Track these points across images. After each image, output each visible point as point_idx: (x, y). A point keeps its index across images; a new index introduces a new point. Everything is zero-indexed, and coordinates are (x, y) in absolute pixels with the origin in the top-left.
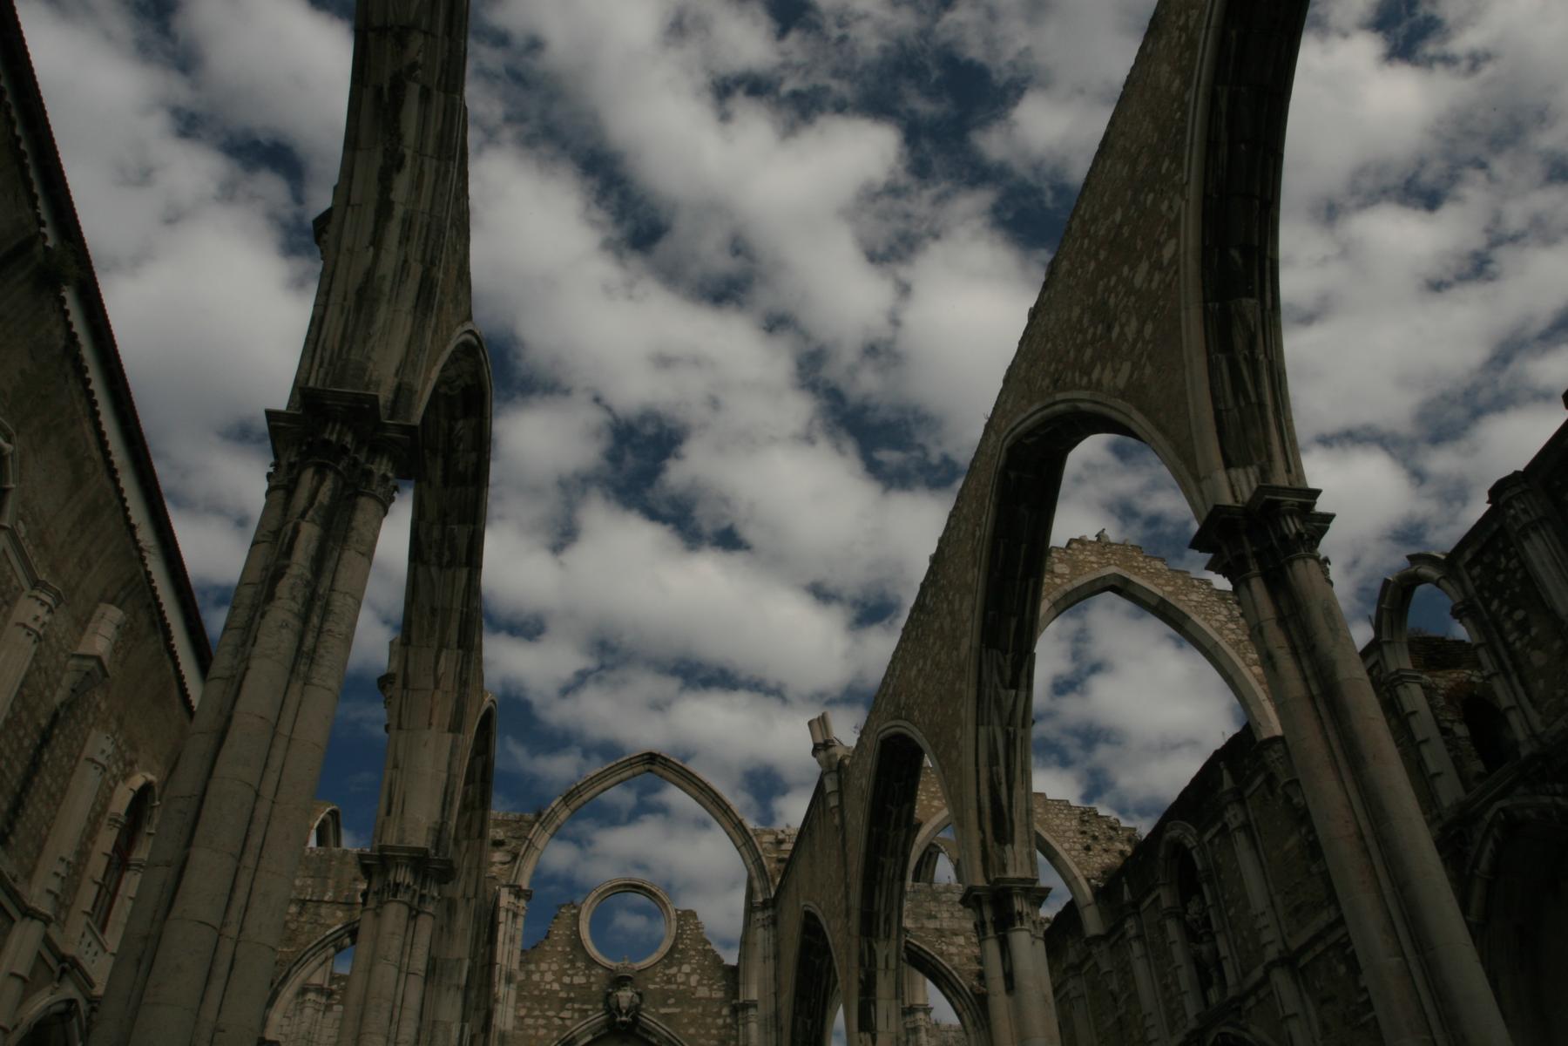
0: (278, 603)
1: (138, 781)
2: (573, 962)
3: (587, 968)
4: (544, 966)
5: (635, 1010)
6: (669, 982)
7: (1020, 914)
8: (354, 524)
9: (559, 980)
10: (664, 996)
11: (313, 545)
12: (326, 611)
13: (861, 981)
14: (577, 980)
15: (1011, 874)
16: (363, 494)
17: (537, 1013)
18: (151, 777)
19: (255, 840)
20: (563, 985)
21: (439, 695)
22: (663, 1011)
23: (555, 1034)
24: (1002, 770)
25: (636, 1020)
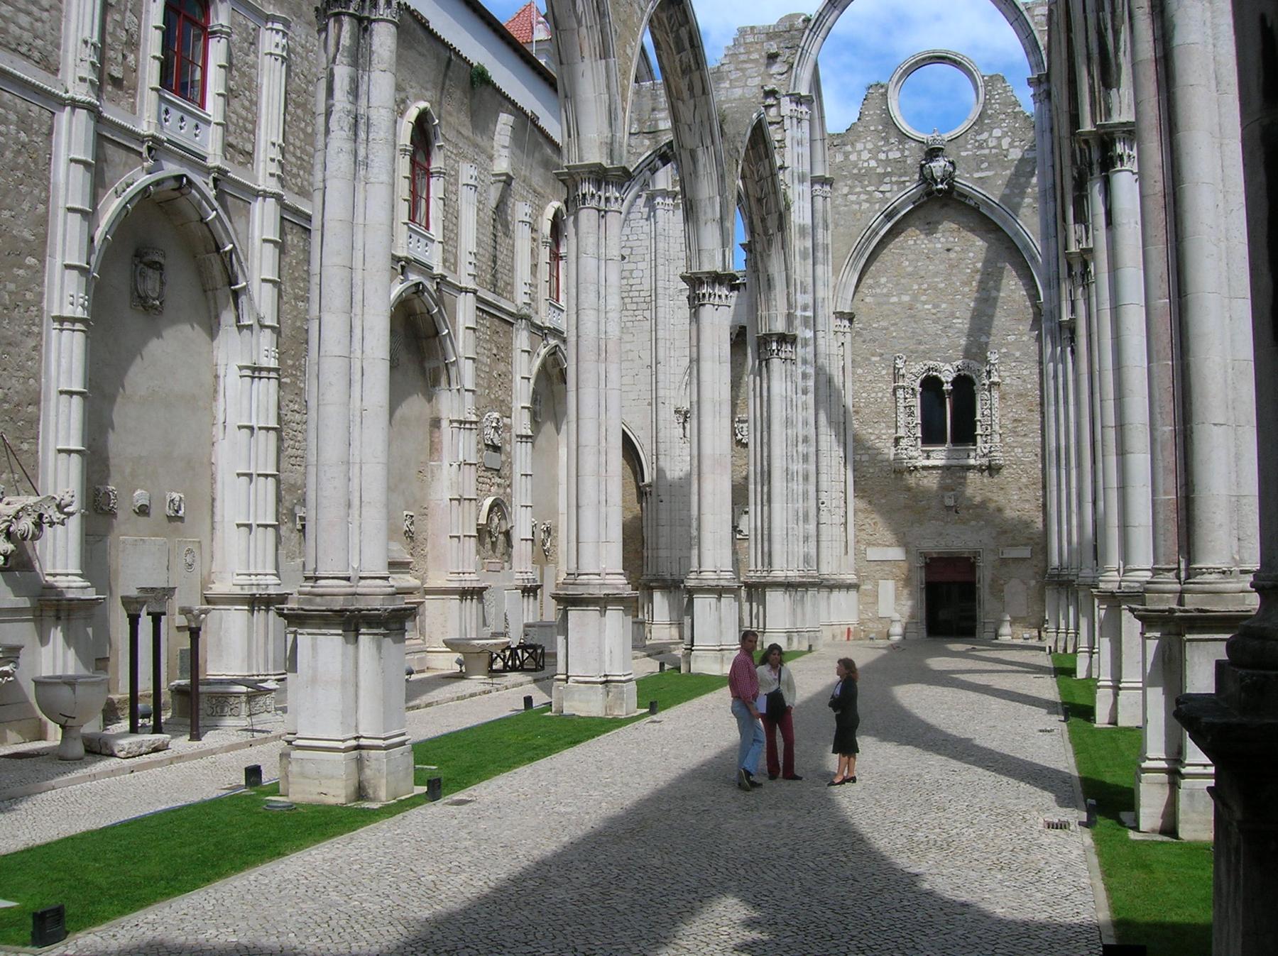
0: (332, 135)
1: (413, 113)
2: (886, 140)
3: (900, 142)
4: (859, 146)
5: (949, 177)
6: (981, 147)
7: (1121, 157)
8: (374, 48)
9: (875, 158)
10: (978, 161)
11: (347, 81)
12: (368, 125)
13: (1074, 178)
14: (891, 156)
15: (1116, 119)
16: (374, 21)
17: (858, 190)
18: (423, 105)
19: (358, 297)
20: (878, 161)
21: (584, 30)
22: (976, 175)
23: (877, 206)
24: (1108, 17)
25: (952, 187)
